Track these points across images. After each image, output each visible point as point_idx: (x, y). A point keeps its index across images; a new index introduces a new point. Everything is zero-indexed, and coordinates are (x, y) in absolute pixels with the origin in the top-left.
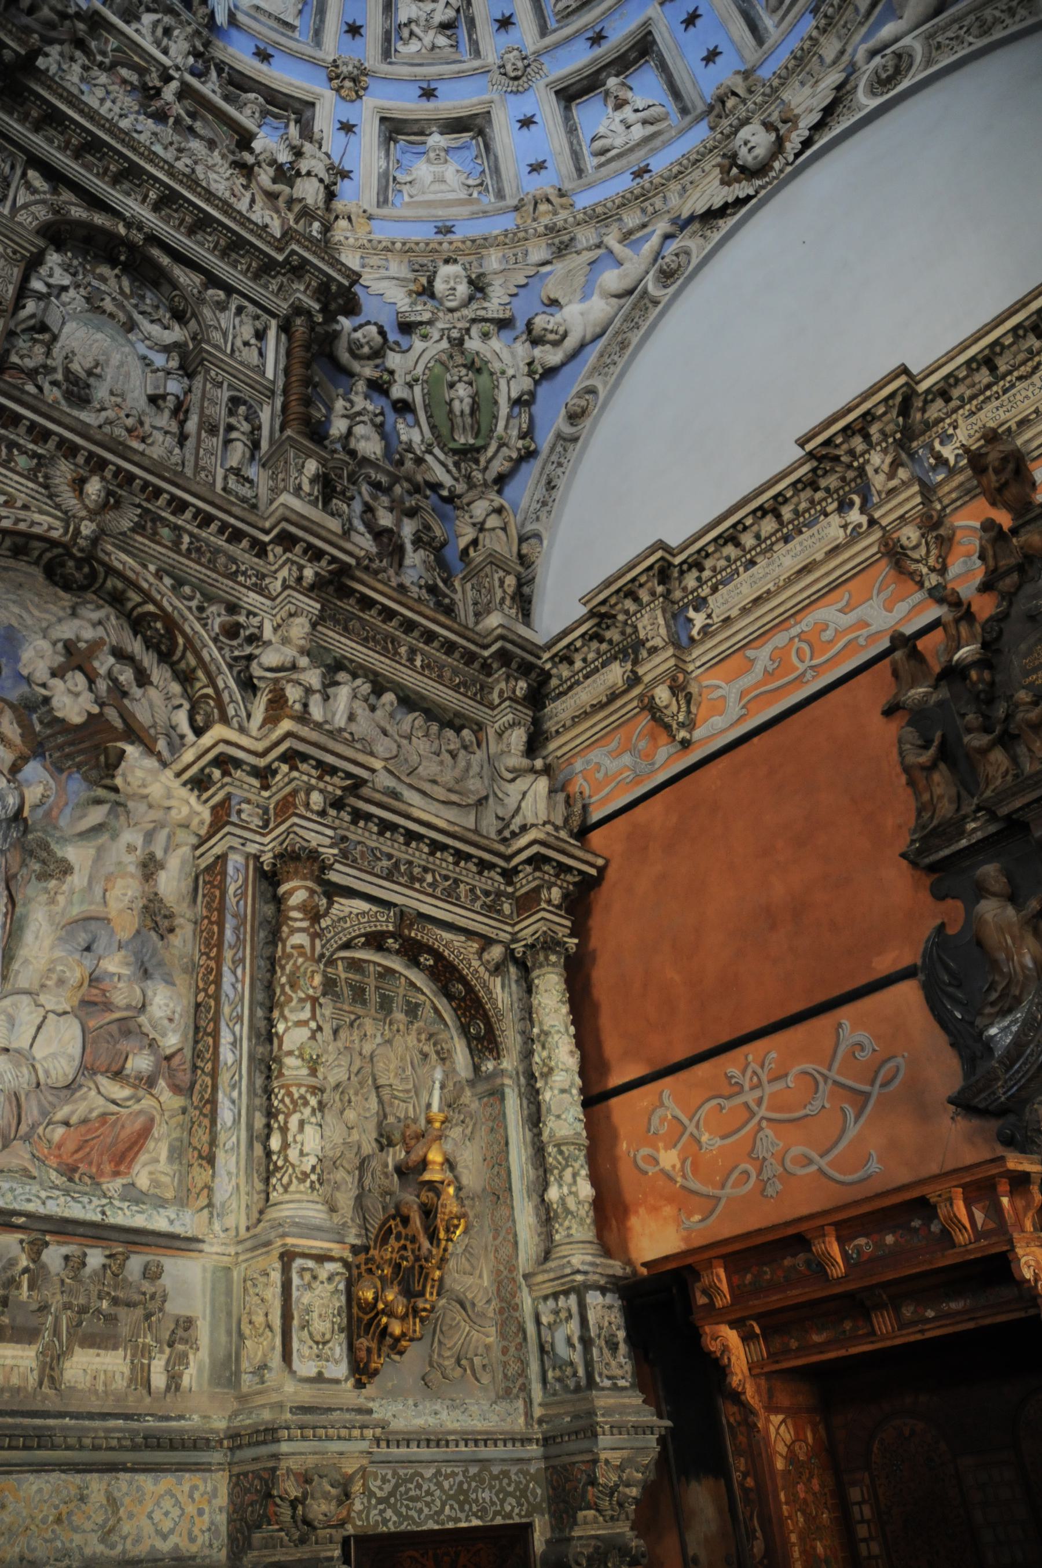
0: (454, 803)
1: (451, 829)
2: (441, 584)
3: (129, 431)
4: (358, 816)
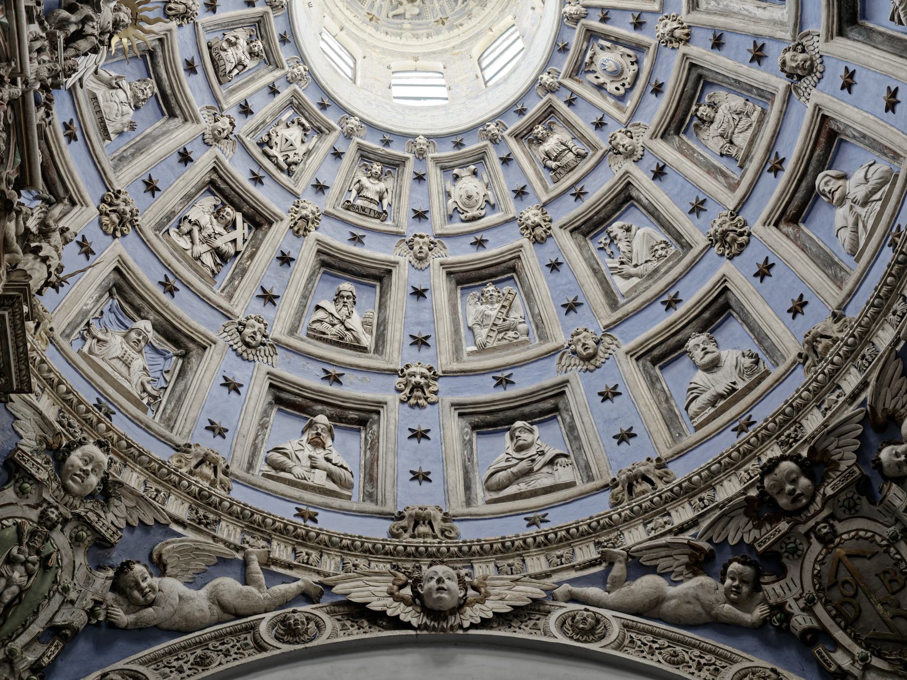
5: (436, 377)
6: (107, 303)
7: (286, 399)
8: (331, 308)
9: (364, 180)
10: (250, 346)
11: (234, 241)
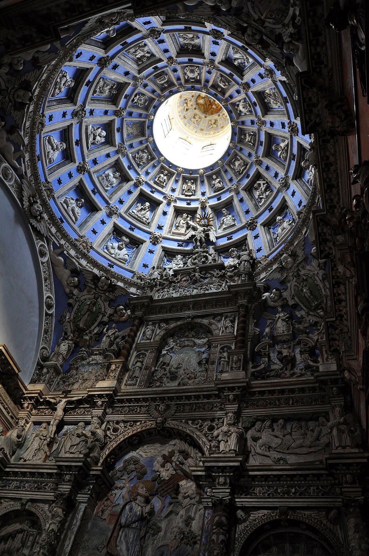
2: (311, 363)
3: (189, 378)
5: (290, 122)
6: (271, 230)
8: (279, 153)
9: (247, 140)
10: (286, 185)
11: (264, 184)
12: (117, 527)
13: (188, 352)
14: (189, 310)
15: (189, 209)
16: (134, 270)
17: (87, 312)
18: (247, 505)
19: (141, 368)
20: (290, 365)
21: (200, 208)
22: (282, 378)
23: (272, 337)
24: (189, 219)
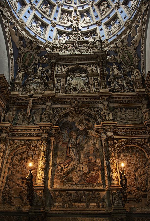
0: (136, 120)
1: (133, 125)
2: (131, 87)
4: (119, 129)
6: (108, 28)
7: (126, 3)
10: (118, 7)
11: (106, 4)
12: (68, 148)
13: (79, 79)
14: (76, 61)
15: (68, 11)
16: (46, 39)
17: (28, 58)
18: (118, 138)
19: (60, 85)
20: (123, 88)
21: (74, 11)
22: (120, 92)
23: (114, 76)
24: (68, 16)
